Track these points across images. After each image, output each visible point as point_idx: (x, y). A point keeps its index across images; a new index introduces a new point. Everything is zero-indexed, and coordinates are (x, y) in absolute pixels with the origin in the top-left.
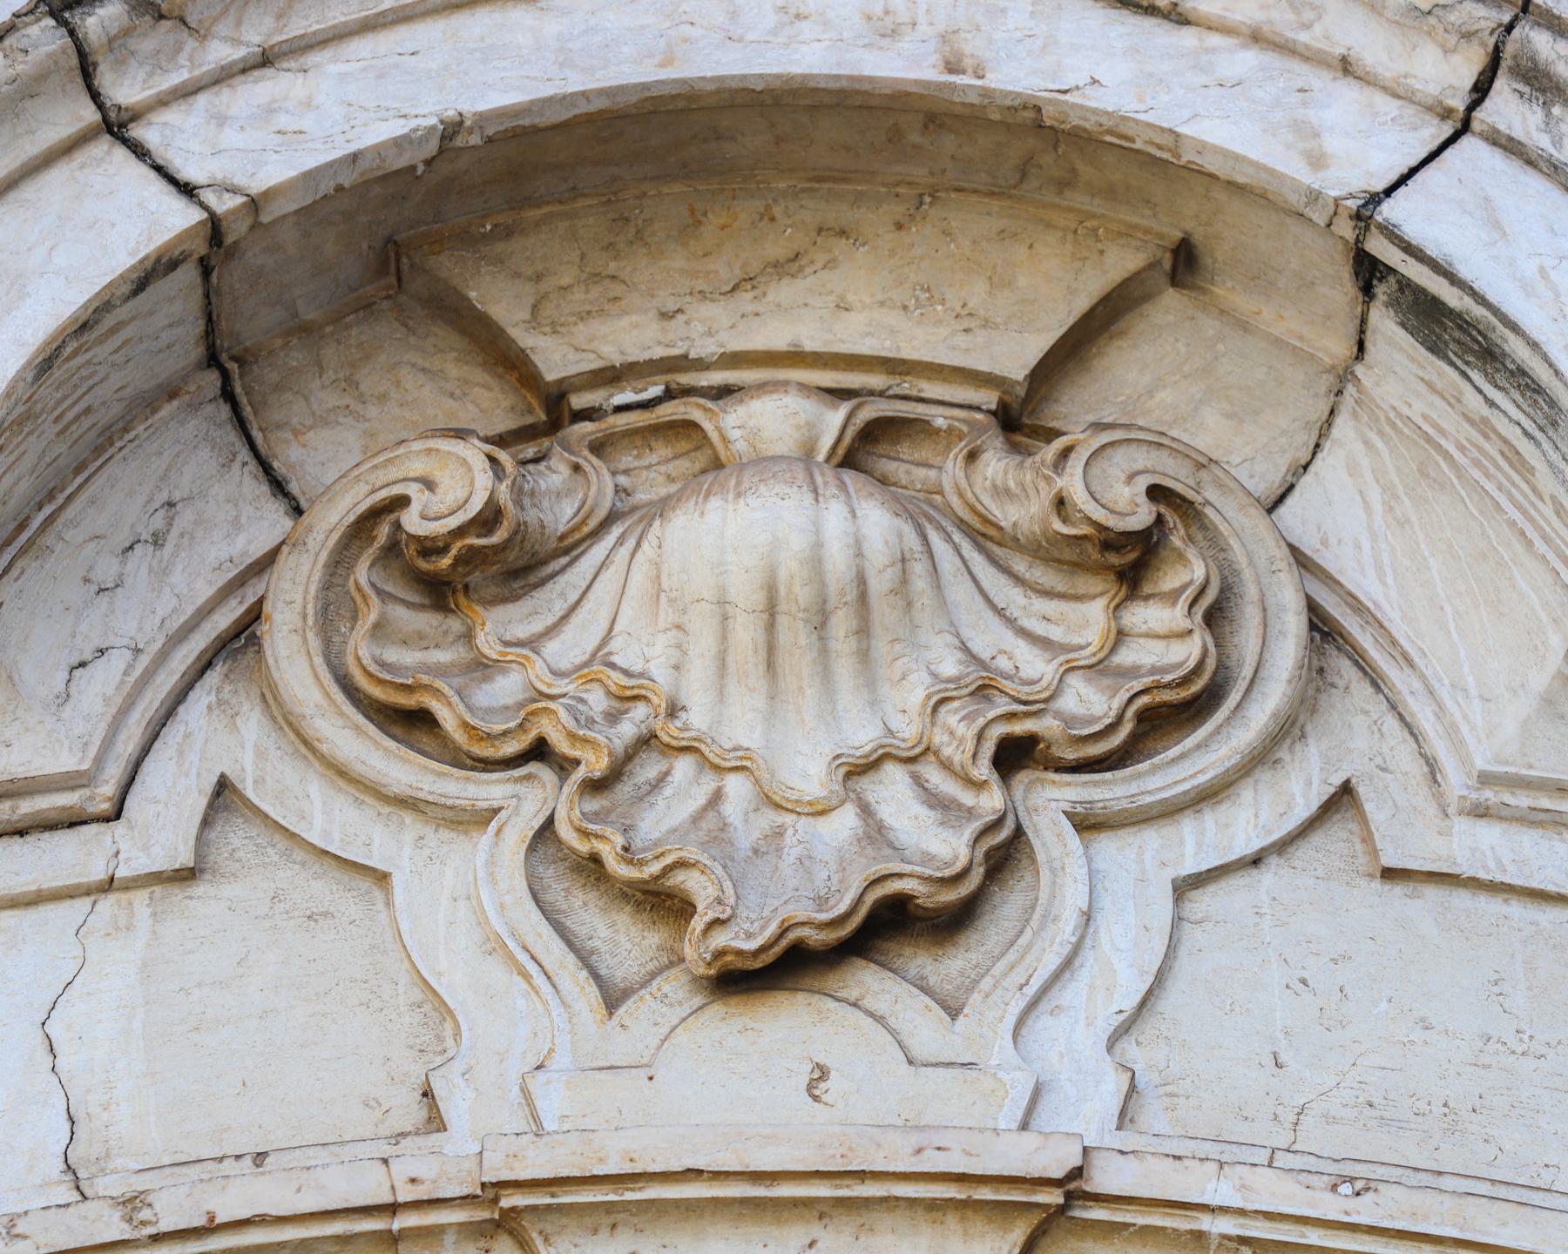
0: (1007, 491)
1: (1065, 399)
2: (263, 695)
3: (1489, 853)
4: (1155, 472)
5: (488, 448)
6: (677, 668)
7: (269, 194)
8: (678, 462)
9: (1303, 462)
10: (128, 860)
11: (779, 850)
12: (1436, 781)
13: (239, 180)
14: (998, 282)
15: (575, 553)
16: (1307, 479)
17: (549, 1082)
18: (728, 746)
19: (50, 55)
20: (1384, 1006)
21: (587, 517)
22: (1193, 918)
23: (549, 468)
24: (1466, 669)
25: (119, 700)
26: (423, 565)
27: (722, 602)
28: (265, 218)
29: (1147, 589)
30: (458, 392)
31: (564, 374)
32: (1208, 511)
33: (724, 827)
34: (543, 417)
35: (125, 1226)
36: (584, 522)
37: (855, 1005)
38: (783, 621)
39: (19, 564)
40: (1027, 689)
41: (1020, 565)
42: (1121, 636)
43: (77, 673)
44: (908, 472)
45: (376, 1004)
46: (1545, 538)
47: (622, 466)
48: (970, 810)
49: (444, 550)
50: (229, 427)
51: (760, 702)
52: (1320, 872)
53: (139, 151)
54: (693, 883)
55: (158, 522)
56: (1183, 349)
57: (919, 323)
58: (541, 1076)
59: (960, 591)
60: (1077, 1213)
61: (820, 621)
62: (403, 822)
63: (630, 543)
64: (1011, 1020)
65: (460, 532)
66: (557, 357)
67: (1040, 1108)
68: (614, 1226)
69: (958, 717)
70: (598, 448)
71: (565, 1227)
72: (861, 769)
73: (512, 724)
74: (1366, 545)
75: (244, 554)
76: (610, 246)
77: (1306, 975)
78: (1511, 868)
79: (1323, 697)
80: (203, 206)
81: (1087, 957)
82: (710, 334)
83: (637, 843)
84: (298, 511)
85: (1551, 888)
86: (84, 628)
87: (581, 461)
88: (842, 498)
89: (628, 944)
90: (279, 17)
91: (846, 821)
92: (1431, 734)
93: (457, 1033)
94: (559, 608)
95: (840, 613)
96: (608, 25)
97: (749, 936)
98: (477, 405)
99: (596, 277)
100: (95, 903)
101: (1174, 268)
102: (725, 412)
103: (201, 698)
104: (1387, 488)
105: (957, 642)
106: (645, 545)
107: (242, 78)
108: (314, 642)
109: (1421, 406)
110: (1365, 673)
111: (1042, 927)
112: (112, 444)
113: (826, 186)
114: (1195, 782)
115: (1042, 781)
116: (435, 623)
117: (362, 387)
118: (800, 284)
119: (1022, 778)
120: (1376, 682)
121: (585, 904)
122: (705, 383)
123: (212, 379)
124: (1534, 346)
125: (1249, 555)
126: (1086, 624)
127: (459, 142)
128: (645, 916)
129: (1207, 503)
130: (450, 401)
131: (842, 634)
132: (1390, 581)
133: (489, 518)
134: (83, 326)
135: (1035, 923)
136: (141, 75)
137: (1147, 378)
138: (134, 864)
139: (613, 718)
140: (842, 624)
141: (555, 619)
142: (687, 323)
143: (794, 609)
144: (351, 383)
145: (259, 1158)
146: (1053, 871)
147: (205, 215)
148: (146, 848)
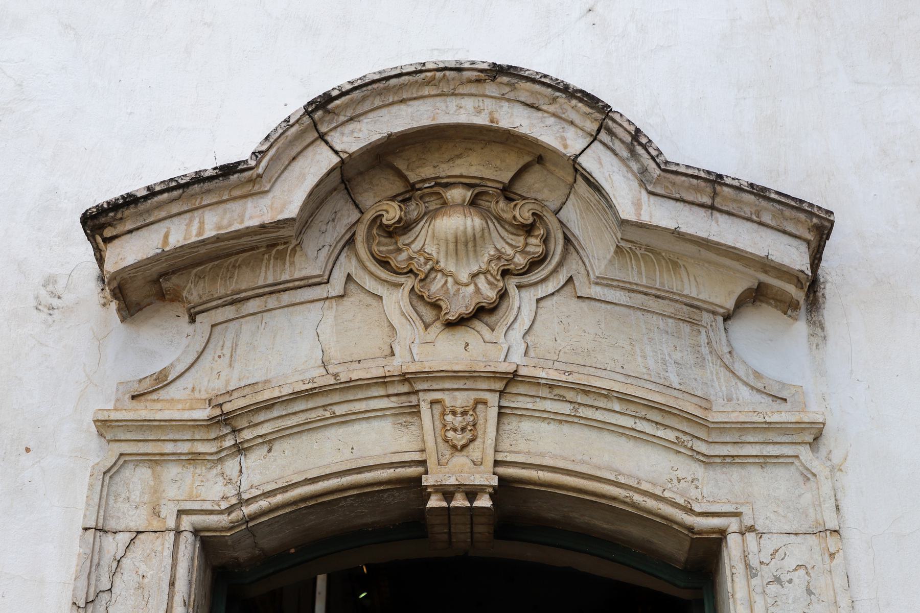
13: (347, 150)
14: (502, 161)
16: (565, 206)
19: (308, 124)
25: (327, 258)
26: (386, 229)
27: (447, 240)
28: (352, 157)
29: (532, 234)
32: (544, 218)
38: (459, 244)
41: (507, 227)
42: (526, 244)
48: (496, 285)
49: (391, 226)
53: (327, 143)
54: (442, 303)
55: (333, 216)
58: (413, 345)
59: (494, 234)
63: (428, 223)
64: (504, 332)
65: (394, 224)
70: (421, 198)
72: (474, 276)
74: (576, 222)
75: (351, 222)
76: (423, 152)
78: (602, 296)
80: (340, 157)
81: (519, 317)
82: (444, 171)
83: (431, 293)
90: (354, 109)
91: (471, 288)
93: (396, 333)
94: (414, 236)
97: (453, 316)
99: (420, 159)
103: (343, 255)
104: (580, 210)
108: (366, 245)
109: (587, 195)
118: (462, 160)
119: (507, 277)
123: (343, 186)
126: (520, 242)
133: (400, 219)
134: (317, 185)
135: (509, 310)
137: (533, 181)
139: (426, 264)
140: (470, 245)
144: (371, 183)
148: (334, 290)
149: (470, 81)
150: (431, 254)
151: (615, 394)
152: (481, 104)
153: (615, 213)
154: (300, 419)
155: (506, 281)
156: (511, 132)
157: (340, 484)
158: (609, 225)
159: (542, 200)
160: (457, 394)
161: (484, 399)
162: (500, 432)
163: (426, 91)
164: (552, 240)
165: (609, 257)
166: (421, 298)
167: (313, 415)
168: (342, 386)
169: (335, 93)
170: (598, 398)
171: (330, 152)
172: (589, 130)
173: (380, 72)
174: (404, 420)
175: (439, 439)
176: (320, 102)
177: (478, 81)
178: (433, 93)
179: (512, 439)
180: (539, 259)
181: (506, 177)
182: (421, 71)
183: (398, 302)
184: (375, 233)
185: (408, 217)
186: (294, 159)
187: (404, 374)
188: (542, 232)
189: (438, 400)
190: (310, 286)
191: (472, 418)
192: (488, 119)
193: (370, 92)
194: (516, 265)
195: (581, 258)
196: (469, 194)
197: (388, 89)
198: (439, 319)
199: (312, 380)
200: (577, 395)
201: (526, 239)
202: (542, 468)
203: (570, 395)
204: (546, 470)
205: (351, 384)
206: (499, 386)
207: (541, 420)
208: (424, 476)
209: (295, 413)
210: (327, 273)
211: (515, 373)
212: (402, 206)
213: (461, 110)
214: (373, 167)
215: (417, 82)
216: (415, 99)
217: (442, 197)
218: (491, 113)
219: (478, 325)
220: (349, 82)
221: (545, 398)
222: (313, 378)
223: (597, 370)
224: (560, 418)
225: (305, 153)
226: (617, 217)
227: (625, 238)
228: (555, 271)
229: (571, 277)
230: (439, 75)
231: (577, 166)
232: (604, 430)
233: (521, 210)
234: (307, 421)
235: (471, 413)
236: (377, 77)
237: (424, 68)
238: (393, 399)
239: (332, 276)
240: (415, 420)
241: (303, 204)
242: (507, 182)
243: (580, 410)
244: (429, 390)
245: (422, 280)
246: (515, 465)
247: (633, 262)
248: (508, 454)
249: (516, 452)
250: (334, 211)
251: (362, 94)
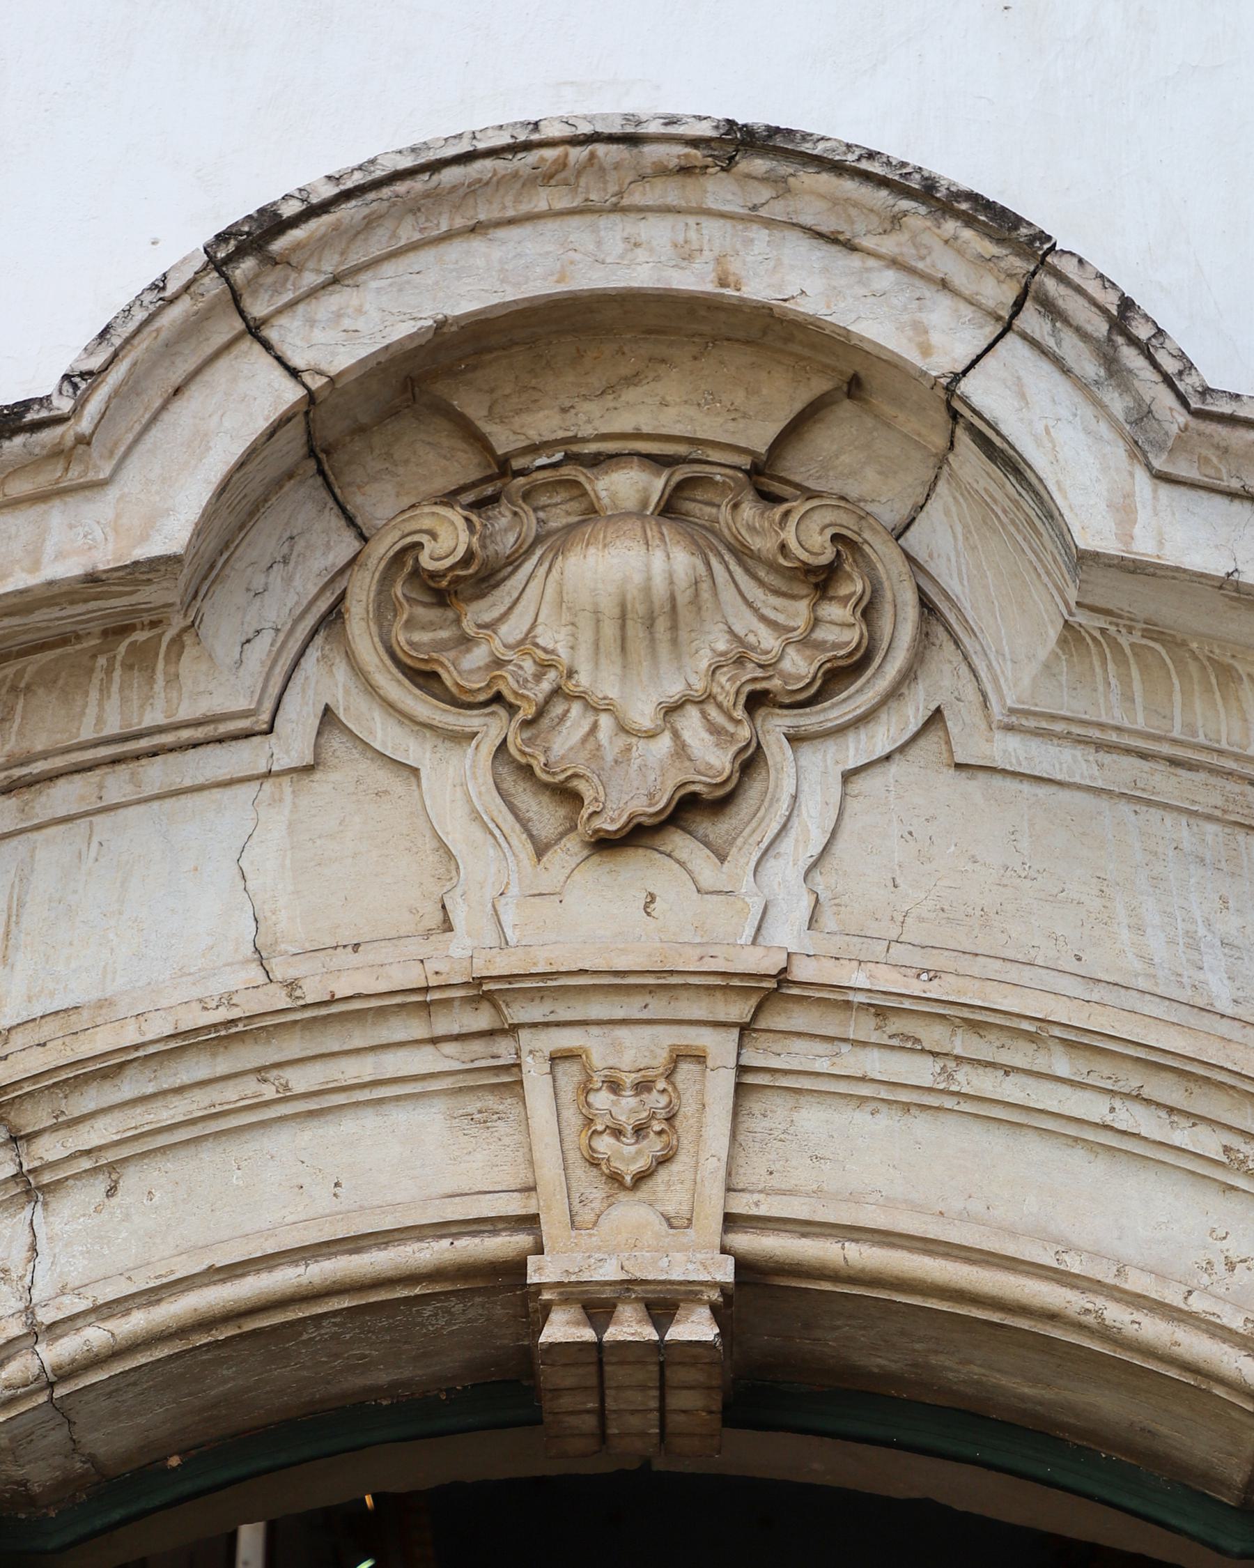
0: (755, 528)
1: (789, 457)
2: (347, 652)
3: (1013, 754)
4: (836, 525)
5: (466, 513)
6: (572, 648)
7: (340, 374)
8: (572, 503)
9: (920, 504)
10: (278, 759)
11: (629, 760)
12: (986, 707)
13: (324, 366)
14: (751, 391)
15: (516, 564)
16: (922, 515)
17: (507, 904)
18: (601, 696)
19: (216, 295)
20: (953, 848)
21: (522, 543)
22: (853, 794)
23: (500, 513)
24: (1004, 643)
26: (432, 584)
27: (596, 612)
28: (338, 386)
29: (831, 593)
30: (449, 455)
31: (507, 450)
32: (866, 547)
33: (599, 747)
34: (497, 471)
36: (520, 547)
37: (669, 856)
38: (630, 623)
39: (212, 590)
40: (764, 657)
41: (762, 574)
42: (816, 622)
43: (246, 646)
44: (701, 510)
45: (415, 850)
47: (541, 503)
48: (732, 735)
49: (444, 576)
50: (322, 489)
51: (618, 670)
52: (922, 764)
53: (267, 346)
54: (581, 786)
55: (285, 549)
56: (855, 433)
57: (707, 414)
58: (503, 900)
59: (728, 594)
61: (650, 622)
62: (425, 736)
63: (546, 565)
64: (753, 864)
65: (452, 568)
66: (503, 438)
67: (767, 916)
69: (726, 678)
70: (526, 496)
72: (672, 710)
73: (483, 684)
74: (953, 559)
75: (333, 565)
77: (911, 829)
78: (1024, 763)
79: (927, 652)
80: (304, 385)
81: (795, 821)
82: (589, 421)
83: (552, 759)
85: (1045, 775)
86: (248, 618)
87: (517, 509)
88: (662, 547)
89: (548, 816)
90: (342, 254)
91: (664, 743)
92: (985, 680)
93: (458, 868)
94: (508, 602)
95: (661, 618)
96: (528, 251)
97: (613, 820)
98: (460, 463)
99: (525, 388)
100: (261, 784)
101: (849, 390)
102: (597, 479)
103: (313, 654)
104: (965, 526)
105: (726, 628)
106: (554, 570)
107: (322, 292)
108: (374, 629)
109: (983, 483)
110: (951, 635)
111: (771, 805)
112: (258, 511)
113: (653, 336)
114: (855, 714)
115: (772, 714)
116: (439, 615)
118: (640, 390)
119: (761, 713)
120: (957, 642)
121: (525, 790)
122: (586, 451)
123: (312, 465)
125: (887, 572)
126: (797, 615)
127: (445, 330)
128: (557, 798)
129: (866, 542)
130: (444, 461)
131: (662, 630)
132: (965, 583)
134: (241, 465)
135: (766, 804)
136: (267, 297)
137: (835, 447)
138: (281, 762)
139: (538, 678)
140: (662, 624)
141: (505, 608)
142: (576, 414)
143: (636, 617)
144: (389, 456)
145: (356, 947)
146: (776, 770)
147: (306, 392)
148: (287, 752)
149: (662, 171)
150: (553, 652)
151: (1057, 1032)
152: (692, 235)
153: (1062, 534)
154: (195, 1106)
155: (759, 722)
156: (776, 311)
157: (304, 1280)
158: (1044, 566)
159: (859, 501)
160: (622, 1033)
161: (697, 1048)
162: (741, 1138)
163: (542, 200)
164: (888, 609)
165: (1043, 654)
166: (526, 771)
167: (230, 1094)
168: (308, 1014)
169: (290, 209)
170: (1008, 1042)
171: (278, 373)
172: (991, 304)
173: (413, 150)
174: (479, 1105)
175: (574, 1156)
176: (248, 234)
177: (685, 170)
178: (559, 205)
179: (773, 1156)
180: (850, 661)
181: (760, 436)
182: (527, 146)
183: (464, 784)
184: (399, 594)
185: (491, 548)
186: (177, 391)
187: (480, 981)
188: (859, 588)
189: (571, 1050)
190: (220, 741)
191: (664, 1100)
192: (712, 276)
193: (386, 204)
194: (786, 677)
195: (966, 658)
196: (657, 484)
197: (434, 196)
198: (574, 828)
199: (228, 1000)
200: (954, 1033)
201: (814, 607)
202: (856, 1236)
203: (933, 1036)
204: (866, 1241)
205: (335, 1009)
206: (740, 1010)
207: (854, 1103)
208: (531, 1259)
209: (179, 1090)
210: (268, 705)
211: (782, 977)
212: (474, 518)
213: (639, 251)
214: (393, 413)
215: (515, 175)
216: (511, 222)
217: (585, 494)
218: (718, 261)
219: (681, 844)
220: (329, 178)
221: (864, 1044)
222: (231, 995)
223: (1009, 964)
224: (904, 1097)
225: (207, 376)
226: (1066, 546)
227: (1087, 601)
228: (894, 694)
229: (938, 711)
230: (577, 154)
231: (957, 405)
232: (1025, 1131)
233: (802, 527)
234: (213, 1110)
235: (661, 1084)
236: (407, 162)
237: (535, 137)
238: (449, 1048)
239: (280, 712)
240: (507, 1104)
241: (203, 515)
242: (762, 449)
243: (960, 1076)
244: (547, 1025)
245: (527, 724)
246: (782, 1227)
247: (1111, 666)
248: (762, 1197)
249: (783, 1193)
250: (287, 534)
251: (366, 211)
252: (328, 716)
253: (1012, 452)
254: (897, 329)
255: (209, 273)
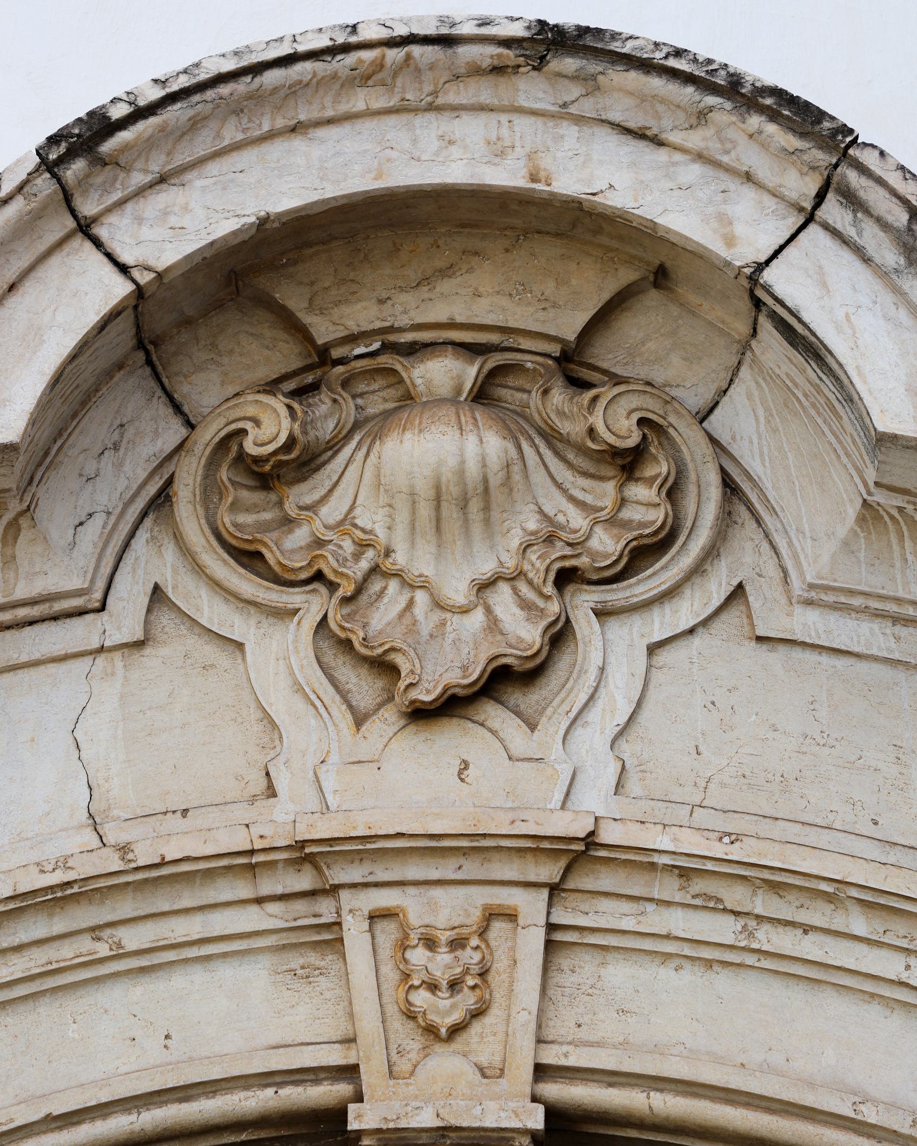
0: (564, 413)
1: (597, 345)
2: (174, 533)
3: (812, 627)
4: (642, 409)
5: (287, 401)
6: (389, 528)
7: (168, 270)
8: (389, 390)
9: (724, 389)
10: (110, 635)
11: (444, 634)
12: (787, 582)
13: (152, 263)
14: (561, 282)
15: (335, 449)
16: (726, 399)
17: (328, 771)
18: (416, 574)
19: (48, 196)
20: (754, 717)
21: (342, 429)
22: (657, 666)
23: (320, 400)
25: (101, 544)
27: (412, 494)
28: (165, 281)
30: (271, 345)
31: (327, 340)
33: (415, 622)
34: (317, 360)
35: (121, 862)
36: (339, 432)
37: (482, 725)
38: (444, 505)
39: (46, 476)
40: (572, 536)
41: (571, 456)
42: (623, 502)
43: (79, 529)
44: (512, 395)
45: (240, 720)
46: (847, 455)
47: (359, 391)
48: (542, 610)
49: (267, 460)
50: (150, 379)
51: (433, 549)
52: (724, 637)
53: (98, 244)
54: (398, 659)
55: (116, 437)
56: (661, 320)
57: (518, 304)
58: (324, 767)
59: (538, 476)
60: (592, 853)
61: (464, 504)
62: (249, 613)
63: (364, 450)
64: (562, 733)
65: (275, 453)
66: (323, 329)
67: (576, 782)
68: (361, 860)
69: (536, 556)
70: (346, 384)
71: (336, 860)
72: (484, 586)
73: (304, 563)
74: (755, 441)
75: (161, 451)
76: (350, 264)
77: (714, 699)
79: (730, 530)
80: (134, 281)
81: (602, 692)
82: (405, 312)
83: (371, 634)
84: (191, 426)
86: (80, 502)
87: (337, 397)
88: (475, 432)
89: (367, 688)
90: (168, 154)
91: (478, 617)
92: (785, 557)
93: (281, 737)
94: (328, 485)
95: (474, 499)
96: (346, 150)
97: (428, 692)
98: (281, 353)
99: (343, 281)
100: (94, 659)
101: (655, 280)
102: (413, 367)
103: (143, 535)
104: (767, 409)
105: (536, 508)
106: (372, 455)
107: (150, 191)
108: (201, 511)
110: (753, 514)
111: (579, 677)
112: (90, 400)
113: (467, 230)
114: (660, 589)
115: (580, 590)
116: (263, 498)
117: (220, 347)
118: (454, 281)
119: (570, 589)
120: (758, 521)
121: (344, 663)
122: (403, 340)
123: (141, 356)
124: (841, 365)
125: (692, 455)
126: (604, 495)
127: (268, 226)
128: (375, 670)
129: (671, 425)
130: (267, 351)
131: (475, 510)
132: (767, 464)
133: (291, 442)
135: (575, 675)
136: (97, 196)
137: (641, 334)
138: (113, 638)
139: (357, 557)
140: (475, 505)
141: (326, 491)
142: (393, 305)
143: (450, 498)
145: (185, 812)
146: (584, 643)
147: (135, 287)
148: (119, 629)
149: (476, 71)
150: (371, 532)
151: (854, 893)
152: (505, 132)
153: (862, 418)
154: (32, 964)
155: (567, 598)
156: (586, 206)
157: (137, 1127)
158: (844, 448)
159: (665, 386)
160: (437, 893)
161: (509, 907)
162: (550, 992)
163: (360, 100)
164: (691, 490)
165: (842, 532)
166: (346, 645)
167: (66, 952)
168: (140, 876)
169: (118, 112)
170: (807, 903)
171: (108, 269)
172: (793, 195)
173: (236, 53)
174: (302, 961)
175: (392, 1010)
176: (79, 136)
177: (498, 70)
178: (376, 105)
179: (581, 1010)
180: (655, 539)
182: (346, 48)
183: (286, 658)
184: (225, 478)
185: (312, 434)
186: (12, 288)
187: (303, 844)
188: (664, 470)
189: (389, 909)
190: (55, 618)
191: (477, 956)
192: (524, 172)
193: (210, 106)
194: (594, 555)
195: (767, 535)
197: (257, 97)
198: (391, 699)
199: (64, 863)
200: (754, 893)
201: (621, 488)
202: (661, 1085)
203: (735, 895)
204: (670, 1091)
205: (165, 871)
206: (549, 871)
207: (658, 960)
208: (352, 1108)
209: (19, 948)
210: (101, 585)
211: (590, 840)
212: (296, 406)
213: (453, 148)
214: (218, 306)
215: (334, 76)
216: (330, 121)
217: (401, 381)
218: (530, 157)
219: (493, 713)
220: (156, 81)
221: (668, 904)
222: (66, 859)
223: (808, 828)
224: (707, 953)
225: (40, 272)
226: (864, 428)
227: (885, 481)
228: (697, 570)
229: (740, 587)
230: (394, 55)
231: (760, 293)
232: (824, 987)
233: (610, 411)
234: (50, 967)
235: (475, 941)
236: (229, 65)
237: (353, 39)
238: (273, 908)
239: (112, 591)
240: (329, 960)
241: (38, 405)
243: (761, 934)
244: (366, 885)
245: (347, 600)
246: (590, 1077)
247: (908, 544)
248: (570, 1048)
249: (591, 1044)
250: (118, 422)
251: (191, 112)
252: (157, 594)
253: (813, 339)
254: (702, 221)
255: (41, 174)
